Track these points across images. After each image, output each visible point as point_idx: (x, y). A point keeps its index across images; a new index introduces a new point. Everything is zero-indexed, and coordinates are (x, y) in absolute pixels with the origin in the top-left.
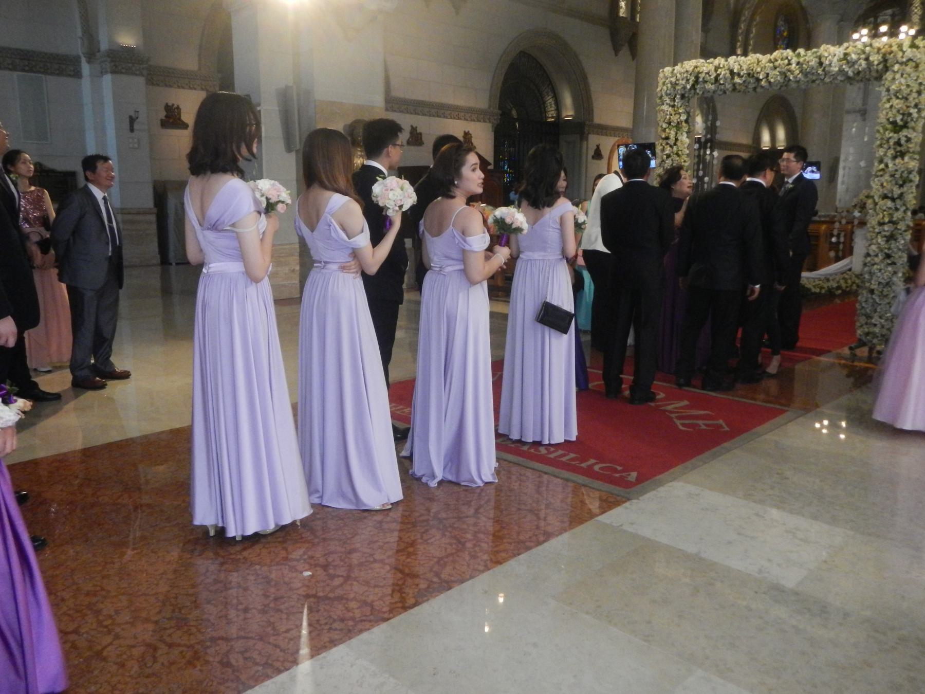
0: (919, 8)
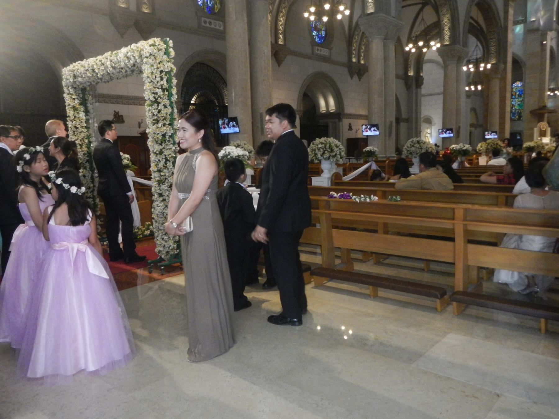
0: (448, 31)
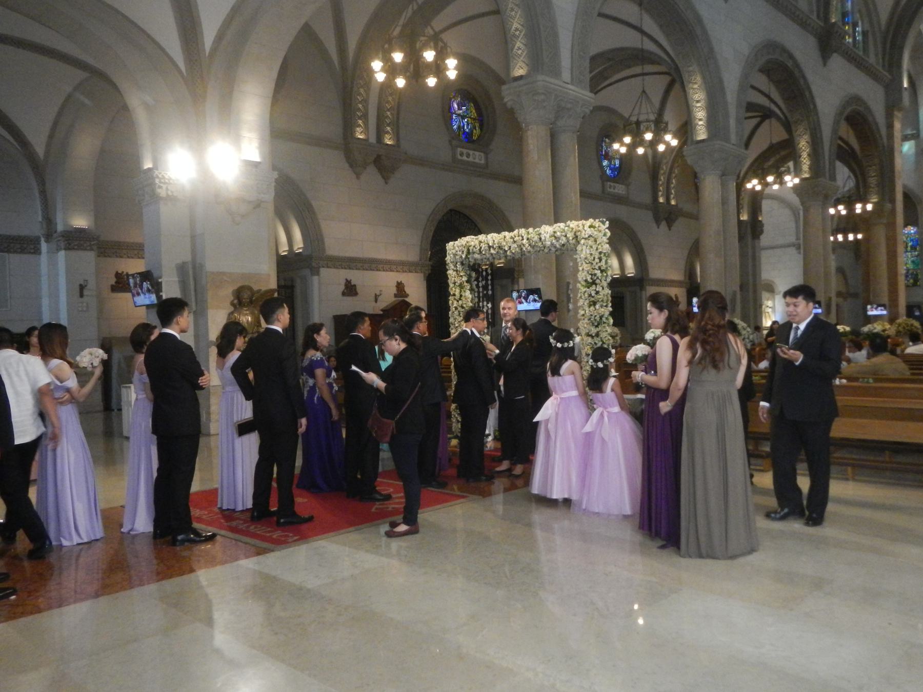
0: (807, 159)
